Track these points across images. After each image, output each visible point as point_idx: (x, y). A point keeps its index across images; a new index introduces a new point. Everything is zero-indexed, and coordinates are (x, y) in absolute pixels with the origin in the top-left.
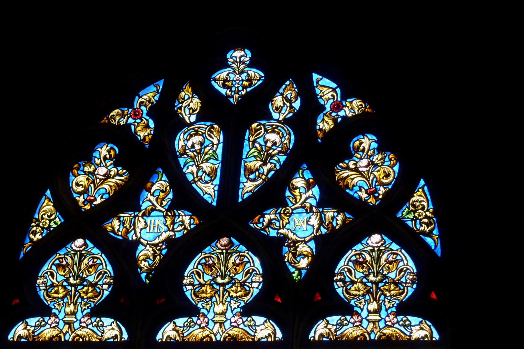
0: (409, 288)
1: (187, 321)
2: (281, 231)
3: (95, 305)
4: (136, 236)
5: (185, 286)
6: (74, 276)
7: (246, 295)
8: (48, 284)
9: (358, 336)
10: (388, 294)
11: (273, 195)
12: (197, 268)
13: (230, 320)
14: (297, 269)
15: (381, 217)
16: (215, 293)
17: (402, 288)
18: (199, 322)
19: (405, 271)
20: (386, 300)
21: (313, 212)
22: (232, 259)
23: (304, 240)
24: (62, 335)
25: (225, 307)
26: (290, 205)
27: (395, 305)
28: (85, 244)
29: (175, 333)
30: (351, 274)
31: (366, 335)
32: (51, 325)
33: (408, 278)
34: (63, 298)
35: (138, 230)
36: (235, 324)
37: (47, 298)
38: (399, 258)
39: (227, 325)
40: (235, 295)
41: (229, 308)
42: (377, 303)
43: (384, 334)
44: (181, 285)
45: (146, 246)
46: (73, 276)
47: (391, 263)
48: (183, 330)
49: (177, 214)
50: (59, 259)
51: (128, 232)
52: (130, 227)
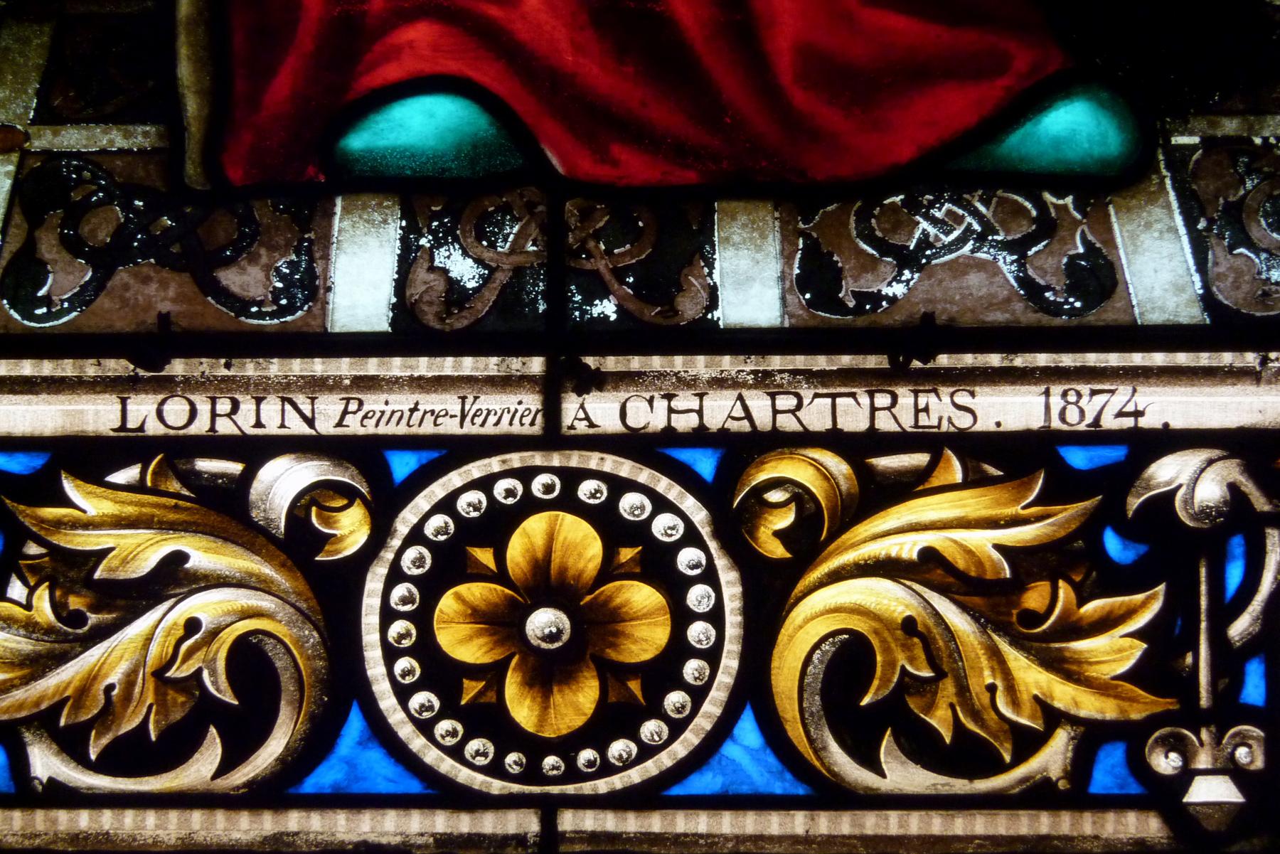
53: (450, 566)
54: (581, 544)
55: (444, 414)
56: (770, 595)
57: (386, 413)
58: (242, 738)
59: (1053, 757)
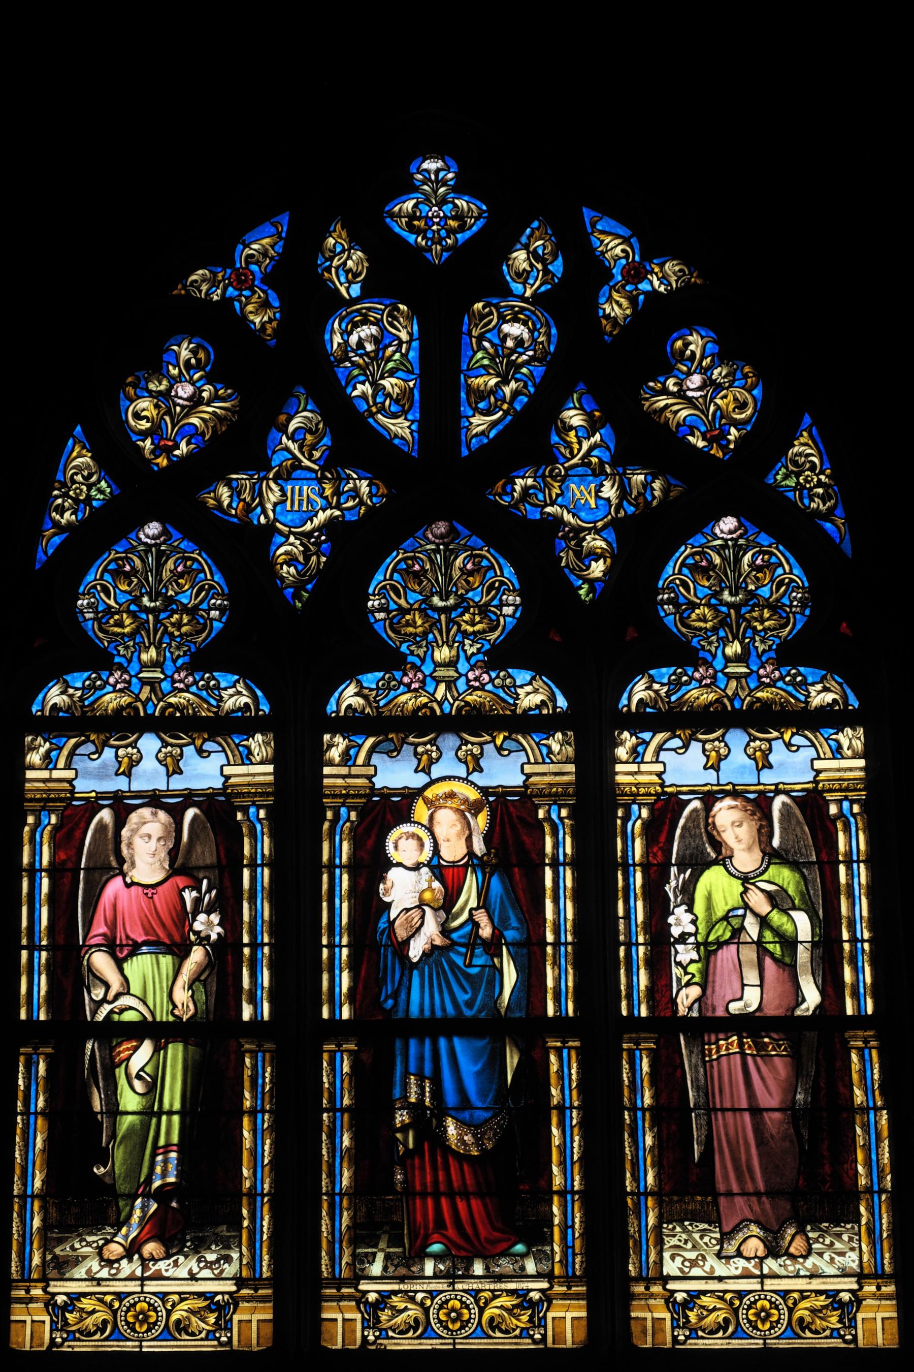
0: (798, 616)
1: (383, 678)
2: (549, 509)
3: (198, 649)
4: (267, 517)
5: (372, 612)
6: (149, 594)
7: (493, 629)
8: (100, 609)
9: (711, 704)
10: (760, 628)
11: (530, 439)
12: (391, 578)
13: (466, 675)
14: (586, 580)
15: (736, 480)
16: (431, 626)
17: (784, 615)
18: (406, 680)
19: (788, 585)
20: (757, 638)
21: (607, 475)
22: (459, 562)
23: (595, 527)
24: (139, 704)
25: (454, 652)
26: (562, 461)
27: (774, 647)
28: (165, 532)
29: (361, 701)
30: (688, 589)
31: (725, 700)
32: (114, 686)
33: (795, 597)
34: (132, 635)
35: (269, 506)
36: (477, 684)
37: (101, 635)
38: (773, 560)
39: (461, 684)
40: (470, 629)
41: (461, 653)
42: (741, 643)
43: (759, 700)
44: (368, 612)
45: (287, 538)
46: (147, 593)
47: (759, 569)
48: (377, 695)
49: (343, 476)
50: (115, 560)
51: (249, 509)
52: (253, 500)
53: (441, 1307)
54: (457, 1304)
55: (440, 1287)
56: (482, 1311)
57: (432, 1287)
58: (416, 1329)
59: (517, 1332)
